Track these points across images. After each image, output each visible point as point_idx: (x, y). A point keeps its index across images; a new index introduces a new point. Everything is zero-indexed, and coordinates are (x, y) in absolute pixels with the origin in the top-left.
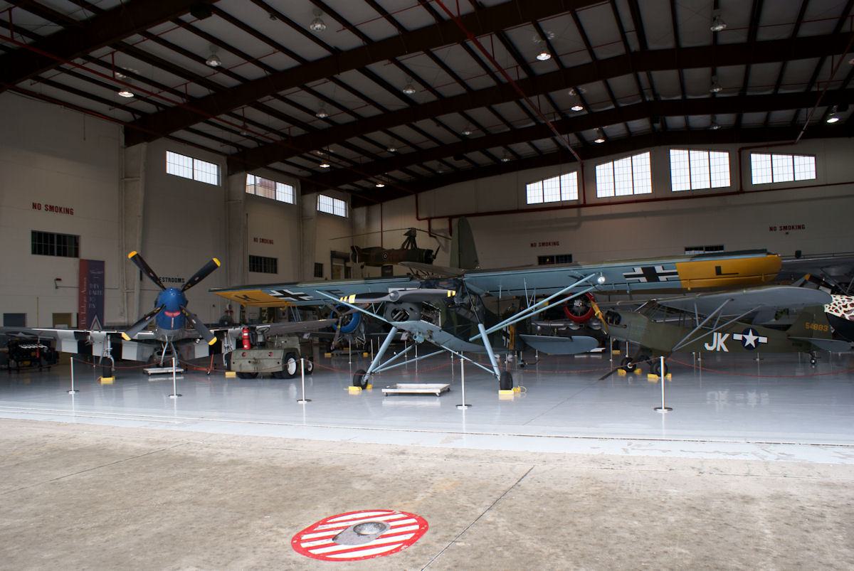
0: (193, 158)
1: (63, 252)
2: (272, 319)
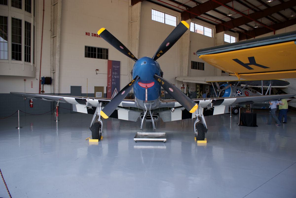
1: (100, 57)
2: (202, 92)
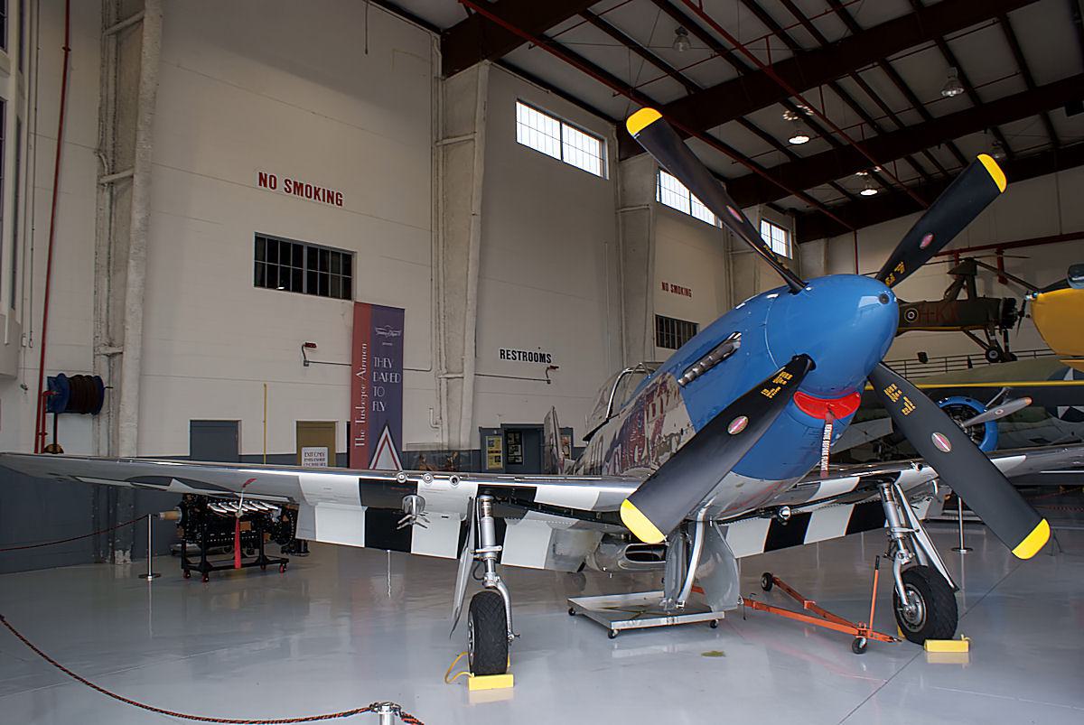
0: (561, 122)
1: (319, 287)
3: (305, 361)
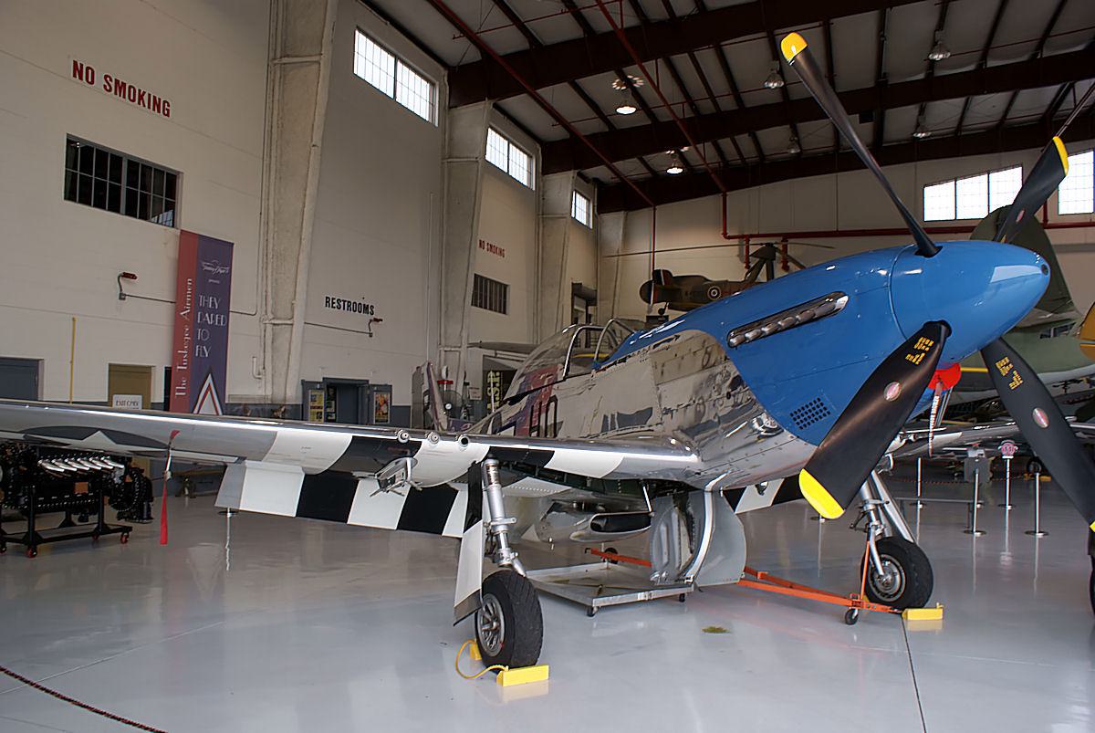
0: (397, 58)
1: (138, 208)
3: (121, 294)
